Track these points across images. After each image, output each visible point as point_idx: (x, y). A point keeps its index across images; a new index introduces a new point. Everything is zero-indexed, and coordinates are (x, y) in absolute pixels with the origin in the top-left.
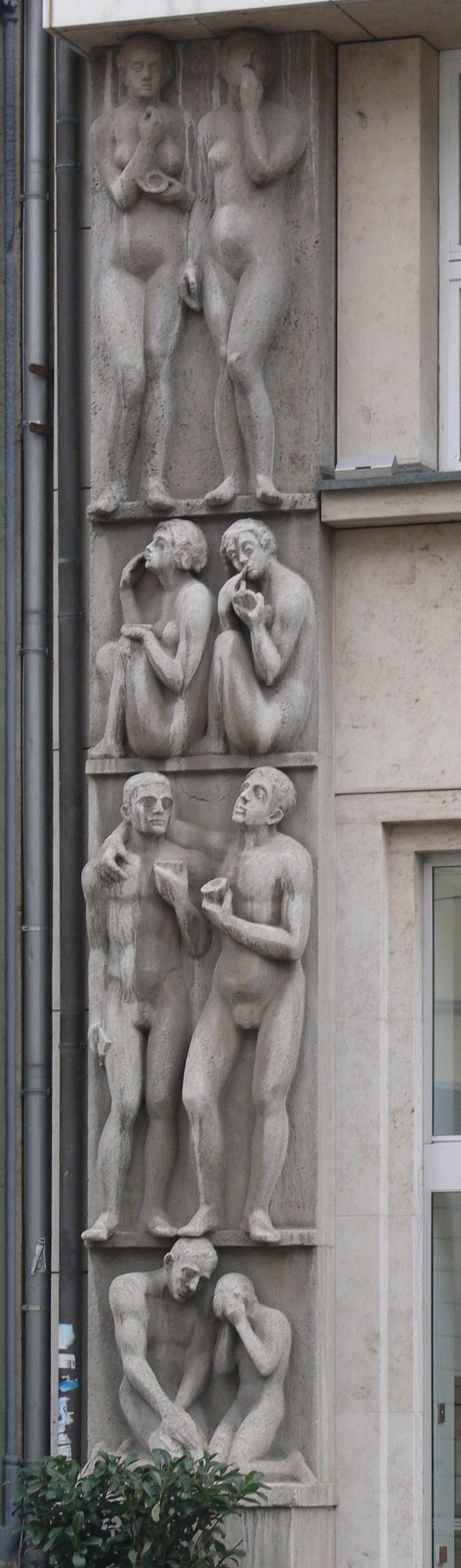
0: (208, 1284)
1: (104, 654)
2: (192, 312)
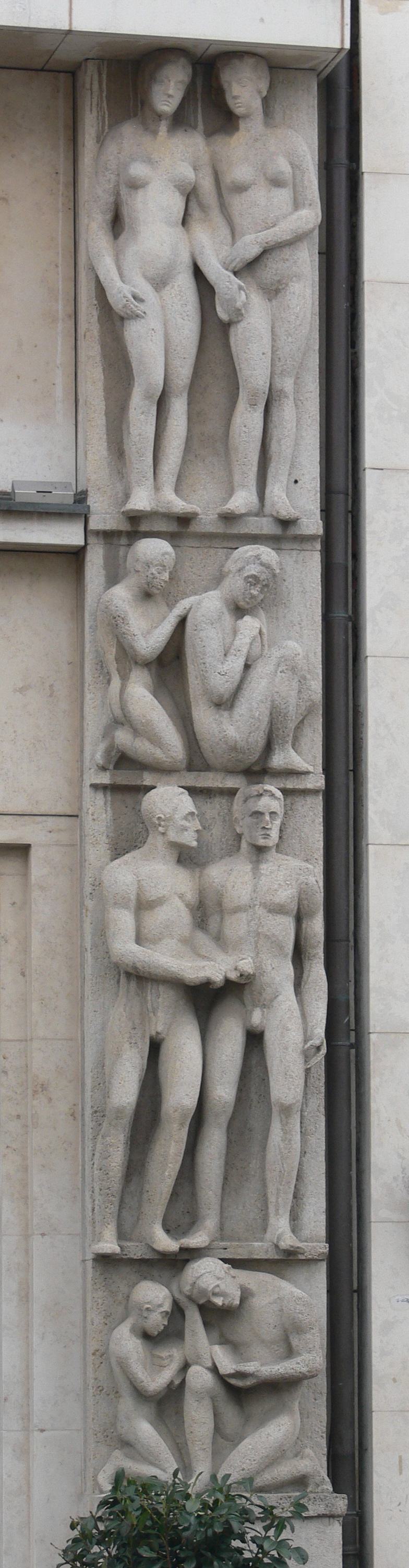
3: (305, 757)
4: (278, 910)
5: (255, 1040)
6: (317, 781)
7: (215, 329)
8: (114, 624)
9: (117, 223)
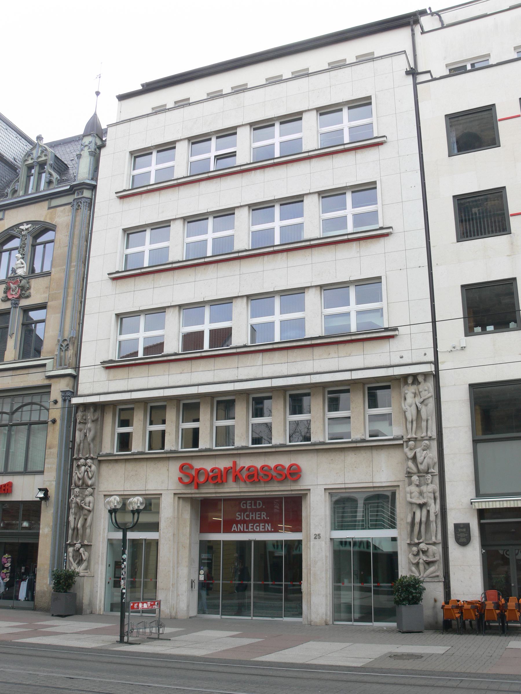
0: (79, 549)
1: (74, 474)
2: (86, 436)
3: (435, 470)
4: (430, 492)
5: (428, 511)
6: (437, 473)
7: (418, 411)
8: (406, 454)
9: (405, 399)
